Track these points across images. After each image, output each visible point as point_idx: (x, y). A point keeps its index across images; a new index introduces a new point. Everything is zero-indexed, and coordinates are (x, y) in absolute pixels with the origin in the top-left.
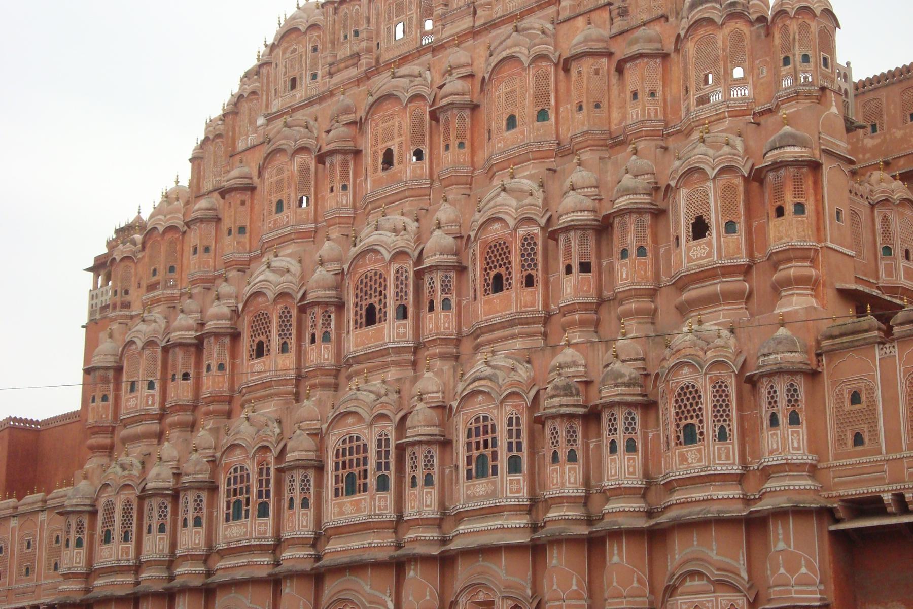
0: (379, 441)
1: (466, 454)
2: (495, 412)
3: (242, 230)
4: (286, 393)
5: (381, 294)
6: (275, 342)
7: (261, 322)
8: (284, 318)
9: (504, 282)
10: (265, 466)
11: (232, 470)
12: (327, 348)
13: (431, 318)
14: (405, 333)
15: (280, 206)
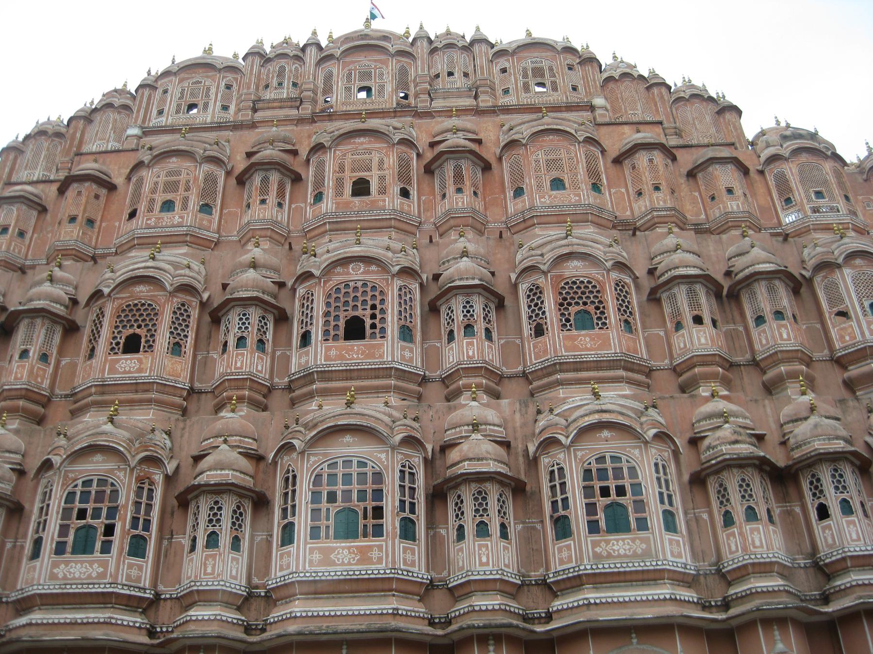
0: (402, 472)
1: (584, 501)
2: (637, 452)
3: (90, 222)
4: (173, 405)
5: (373, 307)
6: (163, 339)
7: (146, 314)
8: (180, 316)
9: (595, 321)
10: (146, 487)
11: (80, 482)
12: (262, 359)
13: (472, 344)
14: (411, 359)
15: (168, 206)
